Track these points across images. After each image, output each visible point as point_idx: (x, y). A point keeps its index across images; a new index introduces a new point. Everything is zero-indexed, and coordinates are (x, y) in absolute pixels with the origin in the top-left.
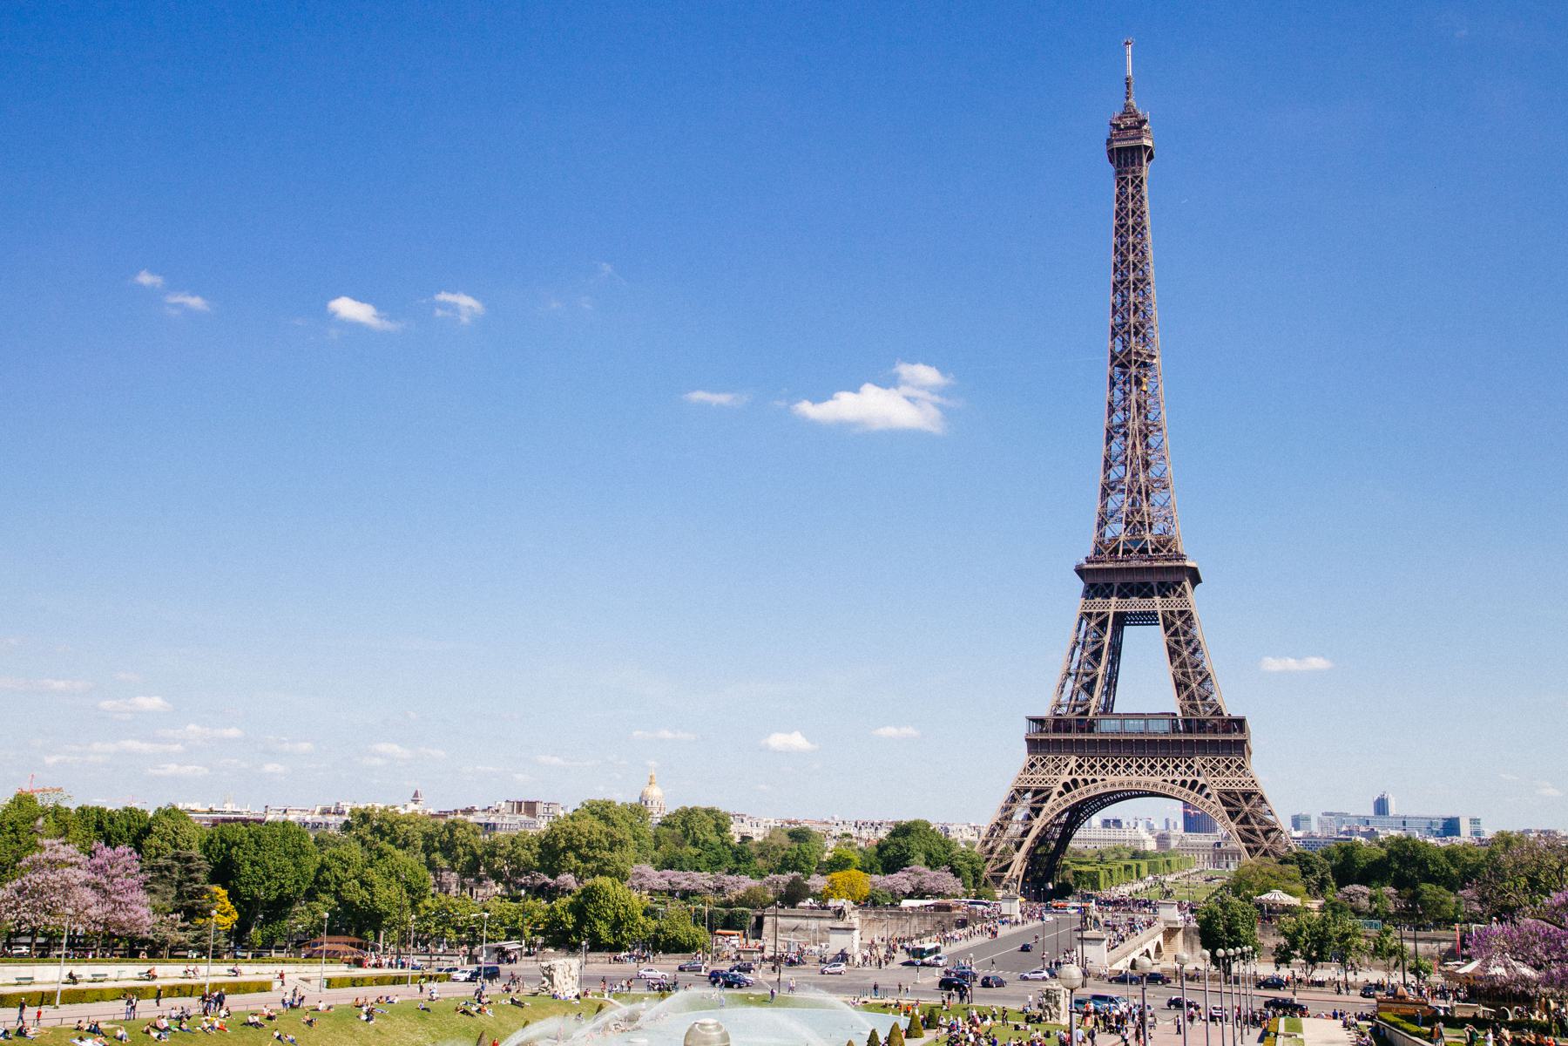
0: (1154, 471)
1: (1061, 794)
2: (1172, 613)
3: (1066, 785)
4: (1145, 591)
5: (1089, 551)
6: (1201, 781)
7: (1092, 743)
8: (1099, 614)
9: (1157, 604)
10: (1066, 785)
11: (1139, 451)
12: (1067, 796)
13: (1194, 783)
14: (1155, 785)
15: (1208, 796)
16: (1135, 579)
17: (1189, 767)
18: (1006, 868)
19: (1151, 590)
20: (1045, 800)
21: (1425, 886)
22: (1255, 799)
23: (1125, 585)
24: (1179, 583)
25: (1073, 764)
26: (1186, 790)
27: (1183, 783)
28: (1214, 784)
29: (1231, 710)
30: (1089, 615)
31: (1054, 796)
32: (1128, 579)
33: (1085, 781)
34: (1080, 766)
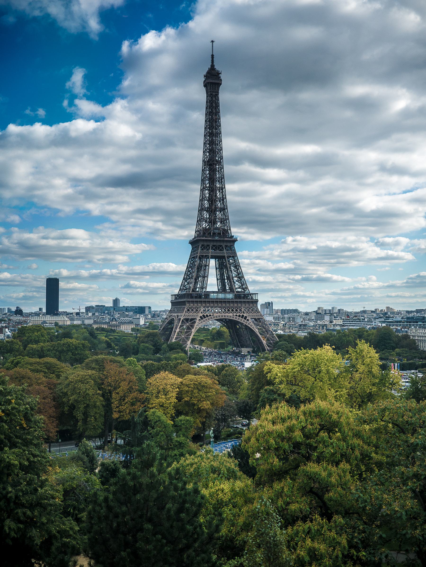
3: (201, 317)
6: (245, 315)
8: (206, 256)
10: (201, 317)
13: (243, 316)
14: (230, 317)
15: (248, 320)
16: (214, 242)
19: (223, 248)
20: (195, 322)
23: (214, 246)
27: (239, 316)
30: (203, 256)
31: (197, 321)
32: (215, 244)
33: (207, 316)
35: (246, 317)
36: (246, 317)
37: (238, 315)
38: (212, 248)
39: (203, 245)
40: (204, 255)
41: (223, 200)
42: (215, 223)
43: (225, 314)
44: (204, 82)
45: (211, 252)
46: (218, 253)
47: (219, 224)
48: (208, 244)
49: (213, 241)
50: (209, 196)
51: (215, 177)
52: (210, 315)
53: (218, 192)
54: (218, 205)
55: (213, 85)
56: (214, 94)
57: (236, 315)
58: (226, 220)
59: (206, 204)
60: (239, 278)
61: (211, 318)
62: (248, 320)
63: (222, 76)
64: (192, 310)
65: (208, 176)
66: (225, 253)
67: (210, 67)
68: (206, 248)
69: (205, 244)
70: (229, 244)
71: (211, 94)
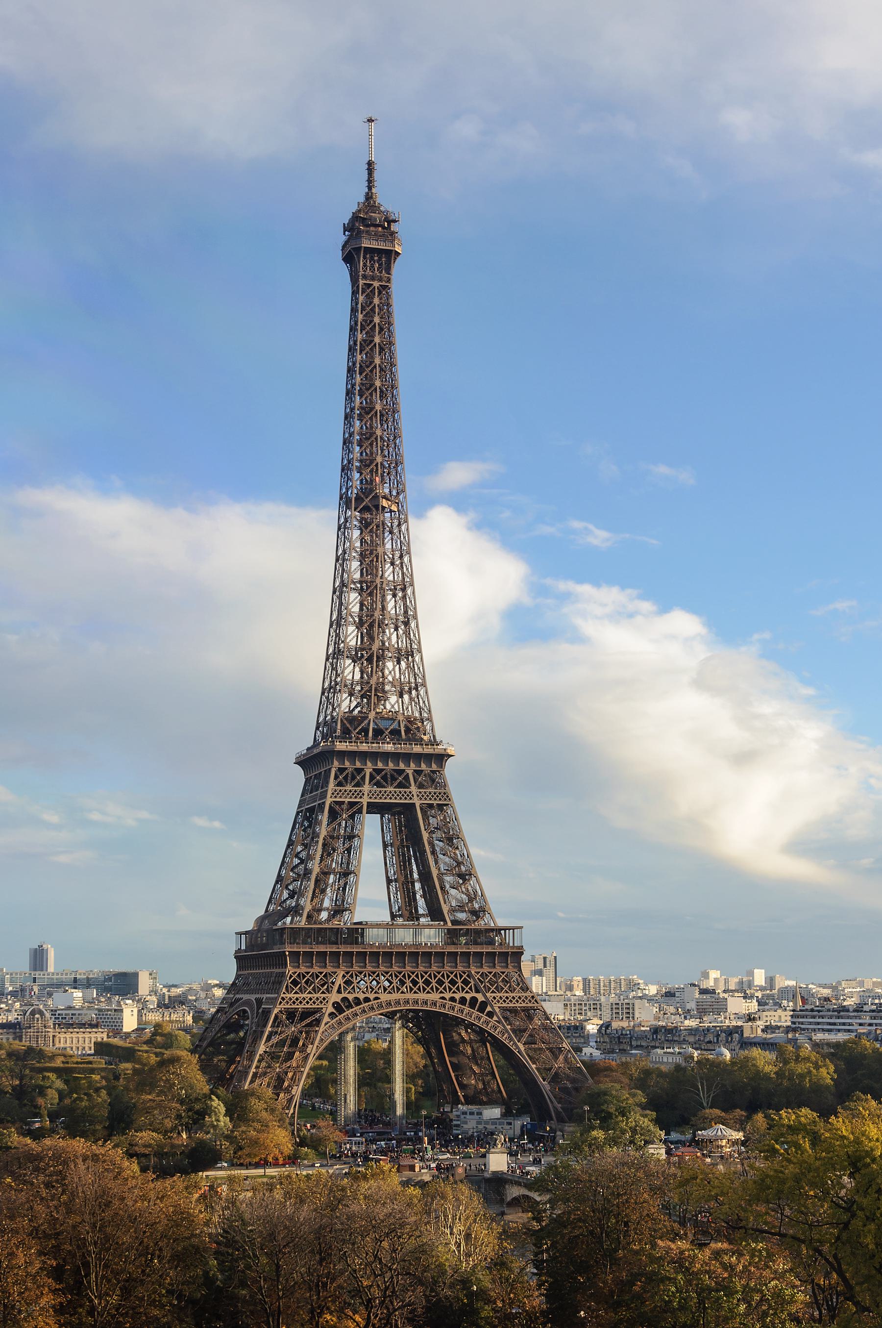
1: (332, 1015)
2: (431, 806)
3: (336, 1006)
6: (480, 998)
7: (362, 955)
8: (352, 804)
10: (336, 1006)
13: (474, 1000)
14: (434, 1004)
19: (407, 777)
20: (318, 1022)
23: (378, 771)
26: (467, 1009)
27: (463, 1001)
28: (497, 1000)
31: (326, 1018)
33: (358, 1002)
35: (484, 1005)
36: (484, 1005)
37: (457, 996)
38: (372, 777)
39: (341, 770)
40: (347, 800)
41: (407, 623)
42: (380, 693)
43: (416, 996)
44: (344, 247)
45: (367, 793)
46: (391, 795)
47: (393, 699)
49: (374, 756)
50: (361, 609)
51: (380, 550)
52: (367, 1000)
53: (389, 597)
54: (389, 639)
55: (372, 259)
56: (376, 284)
57: (453, 999)
58: (416, 689)
59: (352, 636)
60: (461, 876)
61: (372, 1008)
62: (490, 1014)
64: (306, 982)
65: (358, 544)
66: (416, 796)
67: (362, 199)
68: (353, 778)
71: (370, 285)
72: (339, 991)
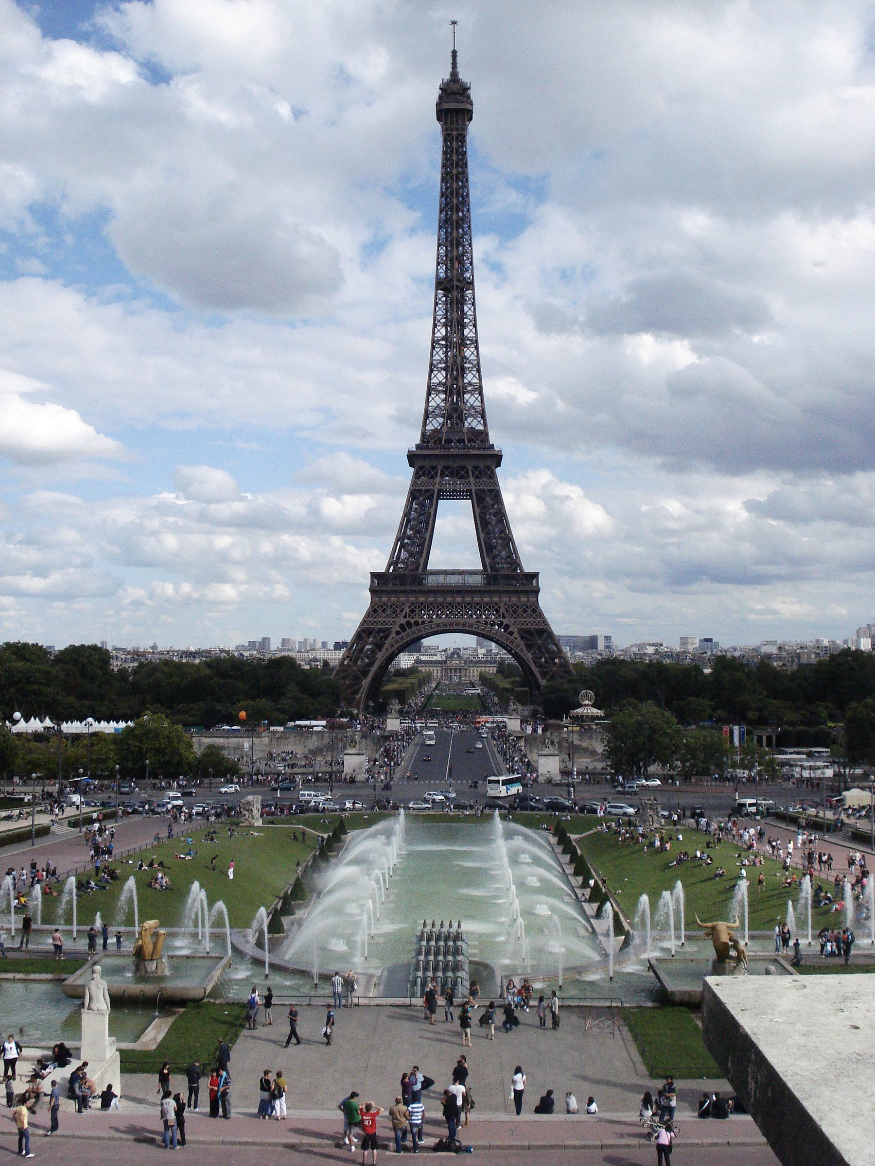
0: (470, 377)
1: (398, 633)
3: (401, 626)
4: (458, 473)
5: (417, 440)
6: (506, 622)
7: (421, 592)
8: (427, 491)
9: (472, 483)
10: (401, 626)
11: (459, 361)
12: (403, 634)
15: (511, 633)
17: (497, 611)
18: (357, 692)
19: (467, 472)
20: (386, 637)
21: (690, 699)
22: (545, 635)
24: (489, 468)
25: (407, 610)
29: (528, 569)
34: (413, 611)
36: (507, 627)
37: (489, 621)
48: (435, 463)
52: (423, 623)
55: (451, 116)
57: (486, 623)
62: (511, 633)
63: (473, 94)
64: (383, 611)
67: (447, 77)
69: (427, 464)
70: (481, 464)
71: (449, 135)
72: (405, 617)
